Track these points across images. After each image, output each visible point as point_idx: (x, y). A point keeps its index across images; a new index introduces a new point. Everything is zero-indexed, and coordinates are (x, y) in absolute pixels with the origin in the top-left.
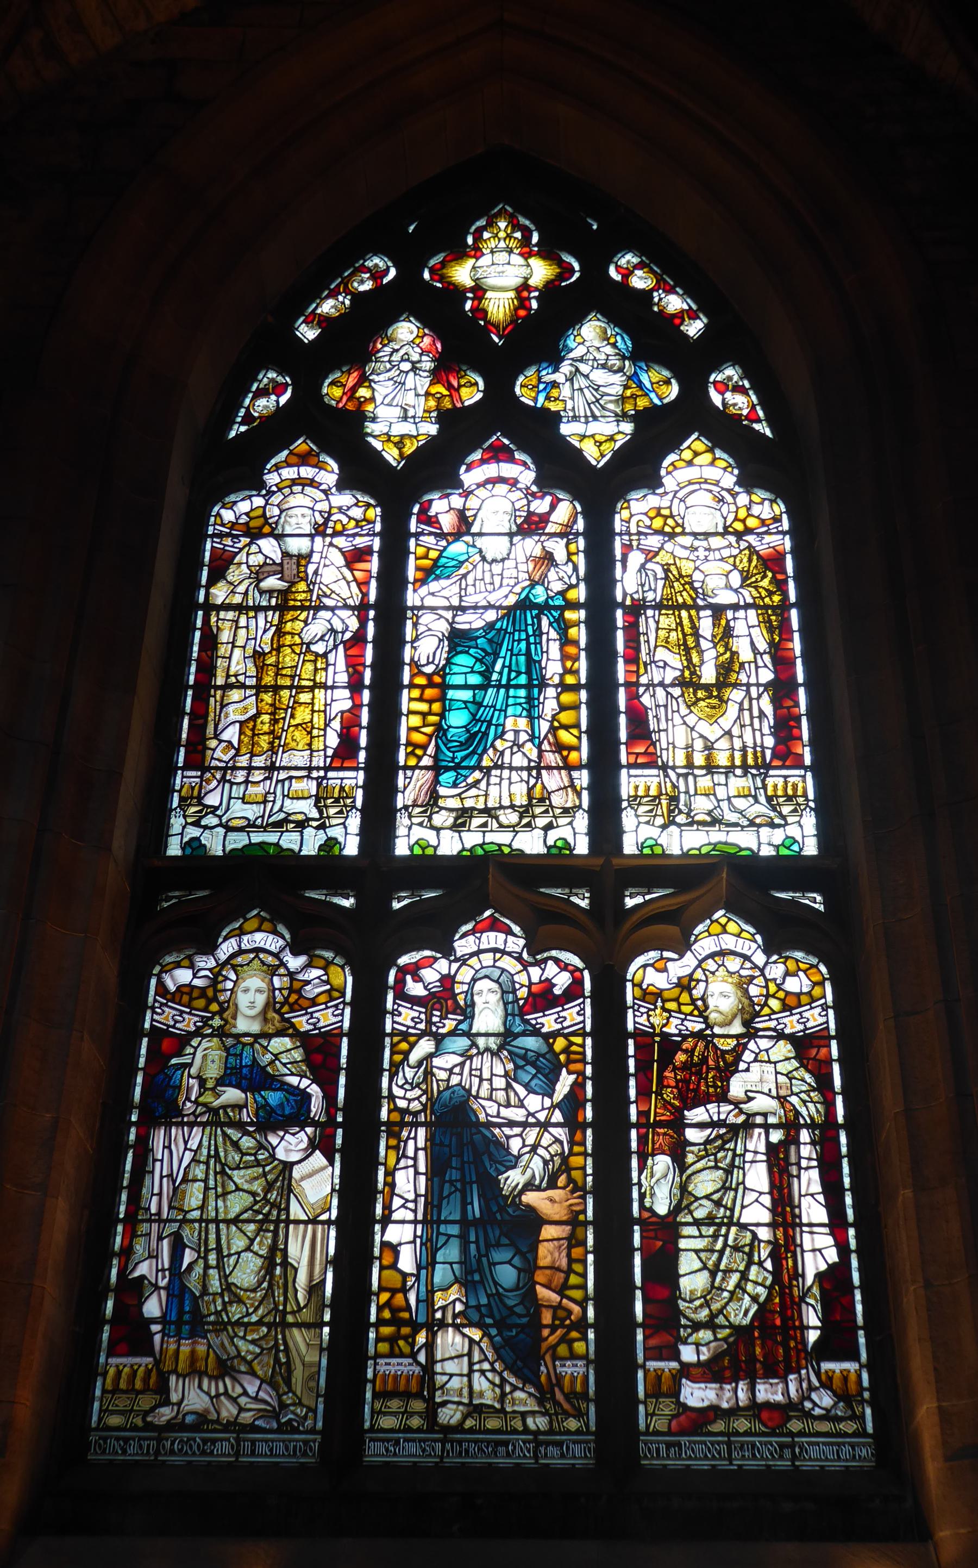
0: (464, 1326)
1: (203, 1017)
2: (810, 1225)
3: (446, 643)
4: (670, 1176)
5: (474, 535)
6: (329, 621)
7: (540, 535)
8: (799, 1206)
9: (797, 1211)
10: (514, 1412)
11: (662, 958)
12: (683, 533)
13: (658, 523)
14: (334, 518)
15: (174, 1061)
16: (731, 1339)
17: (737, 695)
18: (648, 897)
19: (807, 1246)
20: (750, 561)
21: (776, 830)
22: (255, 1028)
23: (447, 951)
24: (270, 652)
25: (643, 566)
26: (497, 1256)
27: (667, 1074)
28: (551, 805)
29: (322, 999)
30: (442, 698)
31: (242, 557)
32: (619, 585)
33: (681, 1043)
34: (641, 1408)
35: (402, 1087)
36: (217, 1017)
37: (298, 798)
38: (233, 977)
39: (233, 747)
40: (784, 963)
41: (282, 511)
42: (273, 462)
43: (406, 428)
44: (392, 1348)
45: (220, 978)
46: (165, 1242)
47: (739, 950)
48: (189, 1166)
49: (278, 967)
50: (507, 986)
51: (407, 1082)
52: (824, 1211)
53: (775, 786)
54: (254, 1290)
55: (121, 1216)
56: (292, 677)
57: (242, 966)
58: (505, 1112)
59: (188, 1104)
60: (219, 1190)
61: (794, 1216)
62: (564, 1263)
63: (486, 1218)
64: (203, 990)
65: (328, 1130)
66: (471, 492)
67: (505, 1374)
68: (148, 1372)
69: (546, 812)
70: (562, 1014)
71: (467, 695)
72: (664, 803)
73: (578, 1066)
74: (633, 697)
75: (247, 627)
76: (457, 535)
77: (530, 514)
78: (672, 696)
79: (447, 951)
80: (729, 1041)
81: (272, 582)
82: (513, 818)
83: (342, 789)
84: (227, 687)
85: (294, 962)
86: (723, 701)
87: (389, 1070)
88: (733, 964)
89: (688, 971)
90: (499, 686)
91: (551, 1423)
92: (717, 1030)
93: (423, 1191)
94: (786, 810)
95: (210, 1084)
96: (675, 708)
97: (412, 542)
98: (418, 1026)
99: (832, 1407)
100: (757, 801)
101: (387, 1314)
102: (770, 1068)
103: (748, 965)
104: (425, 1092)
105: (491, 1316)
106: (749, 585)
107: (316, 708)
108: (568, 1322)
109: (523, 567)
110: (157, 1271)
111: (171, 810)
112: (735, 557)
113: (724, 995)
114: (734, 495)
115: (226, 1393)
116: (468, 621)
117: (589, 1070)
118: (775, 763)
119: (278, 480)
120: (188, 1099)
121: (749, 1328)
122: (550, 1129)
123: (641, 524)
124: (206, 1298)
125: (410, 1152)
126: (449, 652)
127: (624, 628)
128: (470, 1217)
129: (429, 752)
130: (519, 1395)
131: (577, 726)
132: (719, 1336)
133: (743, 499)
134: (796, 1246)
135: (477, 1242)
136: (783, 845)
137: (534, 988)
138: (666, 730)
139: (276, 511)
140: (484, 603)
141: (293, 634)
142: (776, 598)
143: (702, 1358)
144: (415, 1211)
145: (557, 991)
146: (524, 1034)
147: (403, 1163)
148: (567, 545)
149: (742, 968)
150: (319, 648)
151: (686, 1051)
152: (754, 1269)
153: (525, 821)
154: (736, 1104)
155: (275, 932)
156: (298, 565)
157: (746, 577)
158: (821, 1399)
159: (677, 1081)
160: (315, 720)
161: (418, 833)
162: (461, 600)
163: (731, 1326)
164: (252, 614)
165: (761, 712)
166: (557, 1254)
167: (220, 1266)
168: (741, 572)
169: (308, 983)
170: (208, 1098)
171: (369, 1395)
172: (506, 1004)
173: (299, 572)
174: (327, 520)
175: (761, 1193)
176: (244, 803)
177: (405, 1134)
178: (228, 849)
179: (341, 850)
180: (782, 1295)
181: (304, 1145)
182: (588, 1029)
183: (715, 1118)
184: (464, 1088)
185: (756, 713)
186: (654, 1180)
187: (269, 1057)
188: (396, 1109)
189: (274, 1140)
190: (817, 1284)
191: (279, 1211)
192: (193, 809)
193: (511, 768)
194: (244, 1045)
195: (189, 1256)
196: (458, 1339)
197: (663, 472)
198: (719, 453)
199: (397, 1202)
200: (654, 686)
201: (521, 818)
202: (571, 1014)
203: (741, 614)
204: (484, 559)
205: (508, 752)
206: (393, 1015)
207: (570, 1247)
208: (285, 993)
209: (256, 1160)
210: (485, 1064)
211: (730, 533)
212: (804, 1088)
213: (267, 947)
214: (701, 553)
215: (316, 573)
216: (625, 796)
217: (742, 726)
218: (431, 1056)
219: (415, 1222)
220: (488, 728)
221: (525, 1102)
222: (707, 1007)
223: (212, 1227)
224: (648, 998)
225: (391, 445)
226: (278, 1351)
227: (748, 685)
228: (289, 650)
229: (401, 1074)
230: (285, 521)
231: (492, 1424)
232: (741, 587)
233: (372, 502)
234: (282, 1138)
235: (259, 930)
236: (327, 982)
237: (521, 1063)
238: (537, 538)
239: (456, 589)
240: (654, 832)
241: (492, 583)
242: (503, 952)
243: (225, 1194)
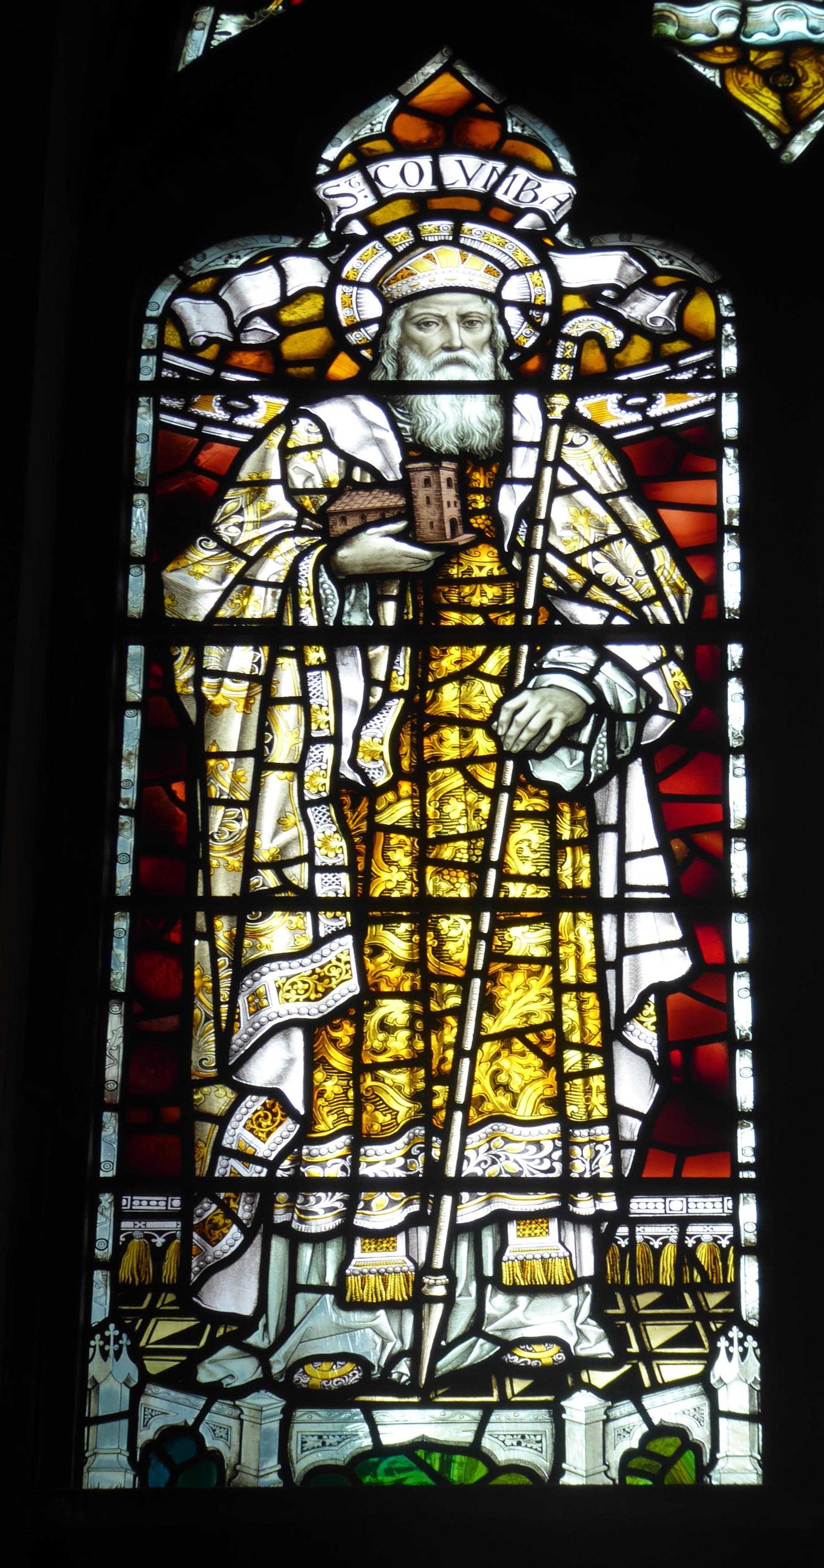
6: (588, 680)
14: (577, 327)
24: (392, 786)
37: (534, 1290)
39: (289, 1111)
41: (390, 306)
75: (303, 700)
107: (569, 976)
111: (90, 1332)
119: (367, 201)
139: (372, 307)
141: (466, 725)
156: (464, 488)
160: (570, 1015)
164: (315, 655)
173: (467, 512)
176: (345, 1303)
178: (302, 1464)
179: (704, 1469)
192: (165, 1329)
225: (751, 80)
228: (457, 780)
230: (406, 340)
233: (701, 272)
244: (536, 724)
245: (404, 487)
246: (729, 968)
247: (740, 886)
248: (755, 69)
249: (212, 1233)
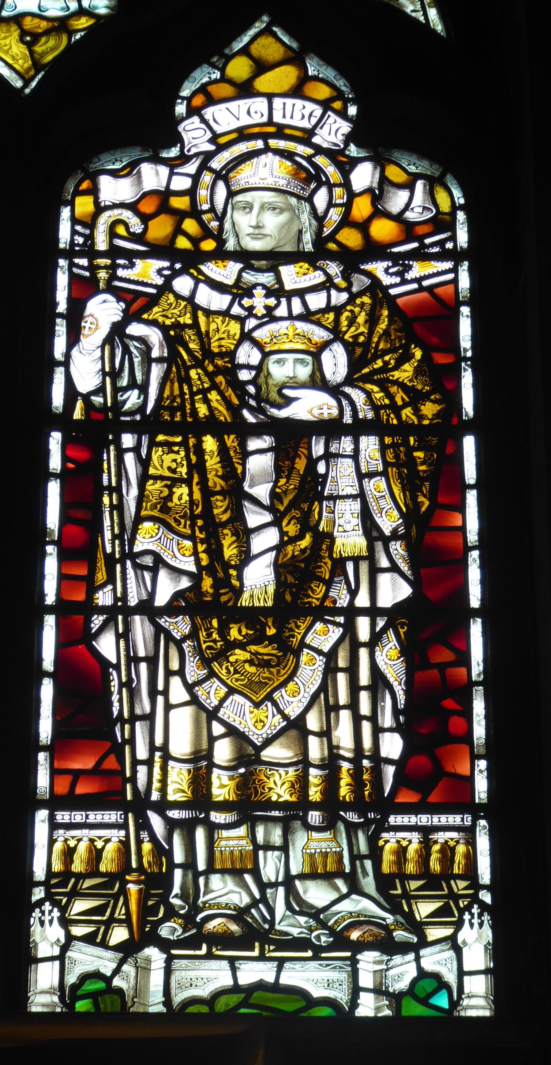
20: (372, 321)
21: (398, 959)
53: (401, 852)
72: (133, 888)
78: (169, 637)
96: (175, 665)
106: (367, 378)
112: (338, 310)
118: (404, 797)
123: (121, 230)
127: (63, 476)
136: (411, 991)
138: (150, 718)
142: (429, 409)
168: (349, 347)
185: (364, 678)
197: (181, 109)
200: (128, 612)
203: (346, 444)
211: (332, 256)
216: (39, 872)
232: (349, 381)
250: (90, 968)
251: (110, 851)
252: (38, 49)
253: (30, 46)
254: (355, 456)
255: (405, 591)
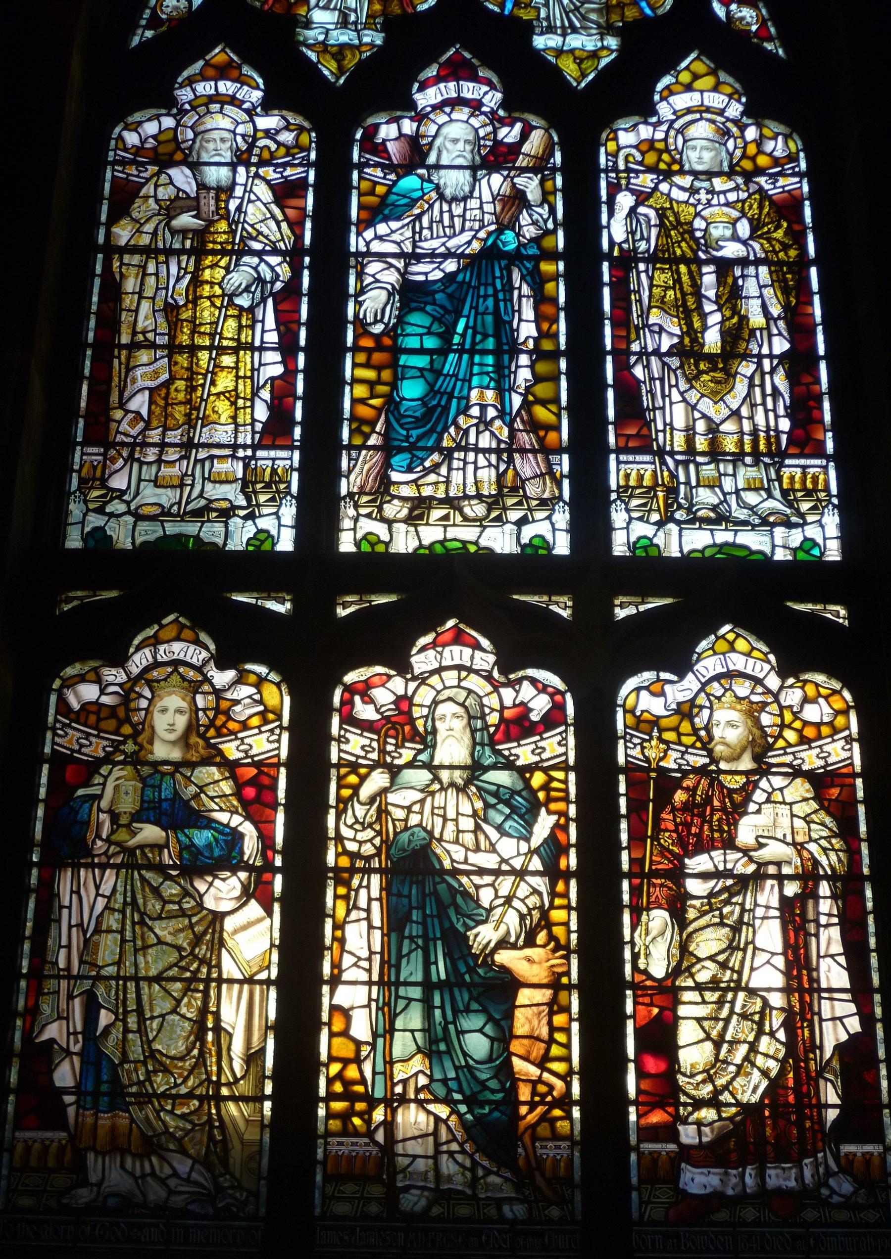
0: (428, 1101)
1: (113, 741)
2: (830, 990)
3: (397, 297)
4: (668, 934)
5: (429, 168)
6: (255, 269)
7: (510, 169)
8: (817, 969)
9: (815, 974)
10: (488, 1198)
11: (658, 680)
12: (682, 172)
13: (651, 158)
14: (261, 143)
15: (81, 792)
16: (738, 1118)
17: (747, 368)
18: (642, 608)
19: (826, 1013)
20: (761, 207)
21: (794, 531)
22: (176, 755)
23: (403, 667)
24: (185, 305)
25: (633, 211)
26: (466, 1023)
27: (664, 816)
28: (525, 495)
29: (255, 721)
30: (394, 364)
31: (149, 189)
32: (605, 233)
33: (680, 780)
34: (634, 1195)
35: (351, 827)
36: (130, 742)
37: (221, 482)
38: (148, 694)
39: (142, 418)
40: (802, 688)
41: (196, 135)
42: (185, 74)
43: (344, 37)
44: (345, 1125)
45: (133, 695)
46: (77, 1002)
47: (749, 671)
48: (102, 914)
49: (202, 683)
50: (475, 710)
51: (357, 821)
52: (845, 974)
53: (792, 478)
54: (182, 1058)
55: (24, 971)
56: (212, 336)
57: (158, 681)
58: (474, 858)
59: (99, 843)
60: (139, 943)
61: (811, 980)
62: (544, 1032)
63: (453, 980)
64: (113, 708)
65: (267, 876)
66: (426, 116)
67: (477, 1156)
68: (62, 1149)
69: (520, 503)
70: (540, 744)
71: (421, 361)
72: (661, 495)
73: (561, 806)
74: (623, 368)
75: (157, 275)
76: (407, 168)
77: (498, 143)
78: (669, 368)
79: (403, 667)
80: (737, 778)
81: (186, 220)
82: (477, 509)
83: (274, 471)
84: (134, 346)
85: (222, 678)
86: (731, 376)
87: (336, 807)
88: (742, 689)
89: (689, 695)
90: (461, 352)
91: (530, 1210)
92: (723, 766)
93: (377, 948)
94: (805, 506)
95: (124, 820)
96: (673, 382)
97: (355, 175)
98: (369, 756)
99: (854, 1193)
100: (770, 496)
101: (338, 1087)
102: (785, 810)
103: (760, 689)
104: (379, 833)
105: (460, 1091)
106: (760, 237)
107: (241, 374)
108: (549, 1099)
109: (488, 208)
110: (69, 1034)
111: (70, 494)
112: (743, 202)
113: (731, 724)
114: (742, 128)
115: (153, 1174)
116: (423, 271)
117: (572, 811)
119: (191, 96)
120: (98, 836)
121: (760, 1105)
122: (528, 878)
123: (631, 159)
124: (126, 1066)
125: (363, 902)
126: (400, 309)
127: (611, 284)
128: (434, 978)
129: (378, 429)
130: (492, 1179)
131: (556, 400)
132: (724, 1115)
133: (751, 133)
134: (813, 1014)
135: (442, 1008)
136: (801, 547)
137: (507, 714)
138: (663, 408)
139: (190, 135)
140: (442, 250)
141: (212, 284)
142: (793, 253)
143: (704, 1139)
144: (369, 971)
145: (535, 717)
146: (494, 767)
147: (354, 915)
148: (542, 183)
149: (752, 693)
150: (244, 301)
151: (687, 789)
152: (765, 1040)
153: (494, 515)
154: (746, 852)
155: (197, 642)
156: (218, 200)
157: (755, 225)
158: (840, 1186)
159: (676, 825)
160: (241, 387)
161: (367, 526)
162: (414, 246)
163: (738, 1104)
164: (162, 258)
165: (774, 388)
166: (536, 1022)
167: (142, 1031)
168: (751, 221)
169: (237, 702)
170: (122, 835)
171: (319, 1178)
172: (473, 732)
173: (218, 208)
174: (251, 146)
175: (773, 954)
176: (156, 486)
177: (355, 882)
178: (139, 540)
179: (274, 544)
180: (796, 1069)
181: (237, 892)
182: (571, 762)
183: (721, 868)
184: (425, 829)
185: (769, 390)
186: (649, 938)
187: (193, 789)
188: (346, 852)
189: (201, 886)
190: (836, 1058)
191: (210, 967)
192: (96, 493)
193: (477, 450)
194: (164, 774)
195: (105, 1018)
196: (422, 1117)
197: (657, 97)
198: (723, 76)
199: (347, 960)
200: (649, 355)
201: (489, 510)
202: (551, 745)
203: (751, 270)
204: (441, 197)
205: (473, 431)
206: (339, 741)
207: (551, 1014)
208: (211, 714)
209: (181, 908)
210: (450, 800)
212: (824, 834)
213: (188, 659)
214: (703, 196)
215: (239, 209)
216: (613, 485)
217: (753, 406)
218: (385, 791)
219: (370, 983)
220: (449, 402)
221: (498, 847)
222: (711, 738)
223: (131, 985)
224: (643, 726)
225: (328, 57)
226: (212, 1127)
227: (760, 357)
228: (208, 303)
229: (350, 812)
230: (201, 146)
231: (464, 1211)
232: (751, 237)
233: (306, 124)
234: (211, 884)
235: (178, 639)
236: (261, 702)
237: (493, 801)
238: (505, 173)
239: (409, 234)
240: (648, 530)
241: (452, 226)
242: (470, 670)
243: (145, 948)
244: (236, 284)
245: (197, 199)
246: (297, 371)
247: (302, 342)
248: (330, 53)
249: (113, 460)
250: (642, 534)
251: (648, 476)
252: (583, 66)
253: (579, 65)
254: (757, 276)
255: (787, 346)
